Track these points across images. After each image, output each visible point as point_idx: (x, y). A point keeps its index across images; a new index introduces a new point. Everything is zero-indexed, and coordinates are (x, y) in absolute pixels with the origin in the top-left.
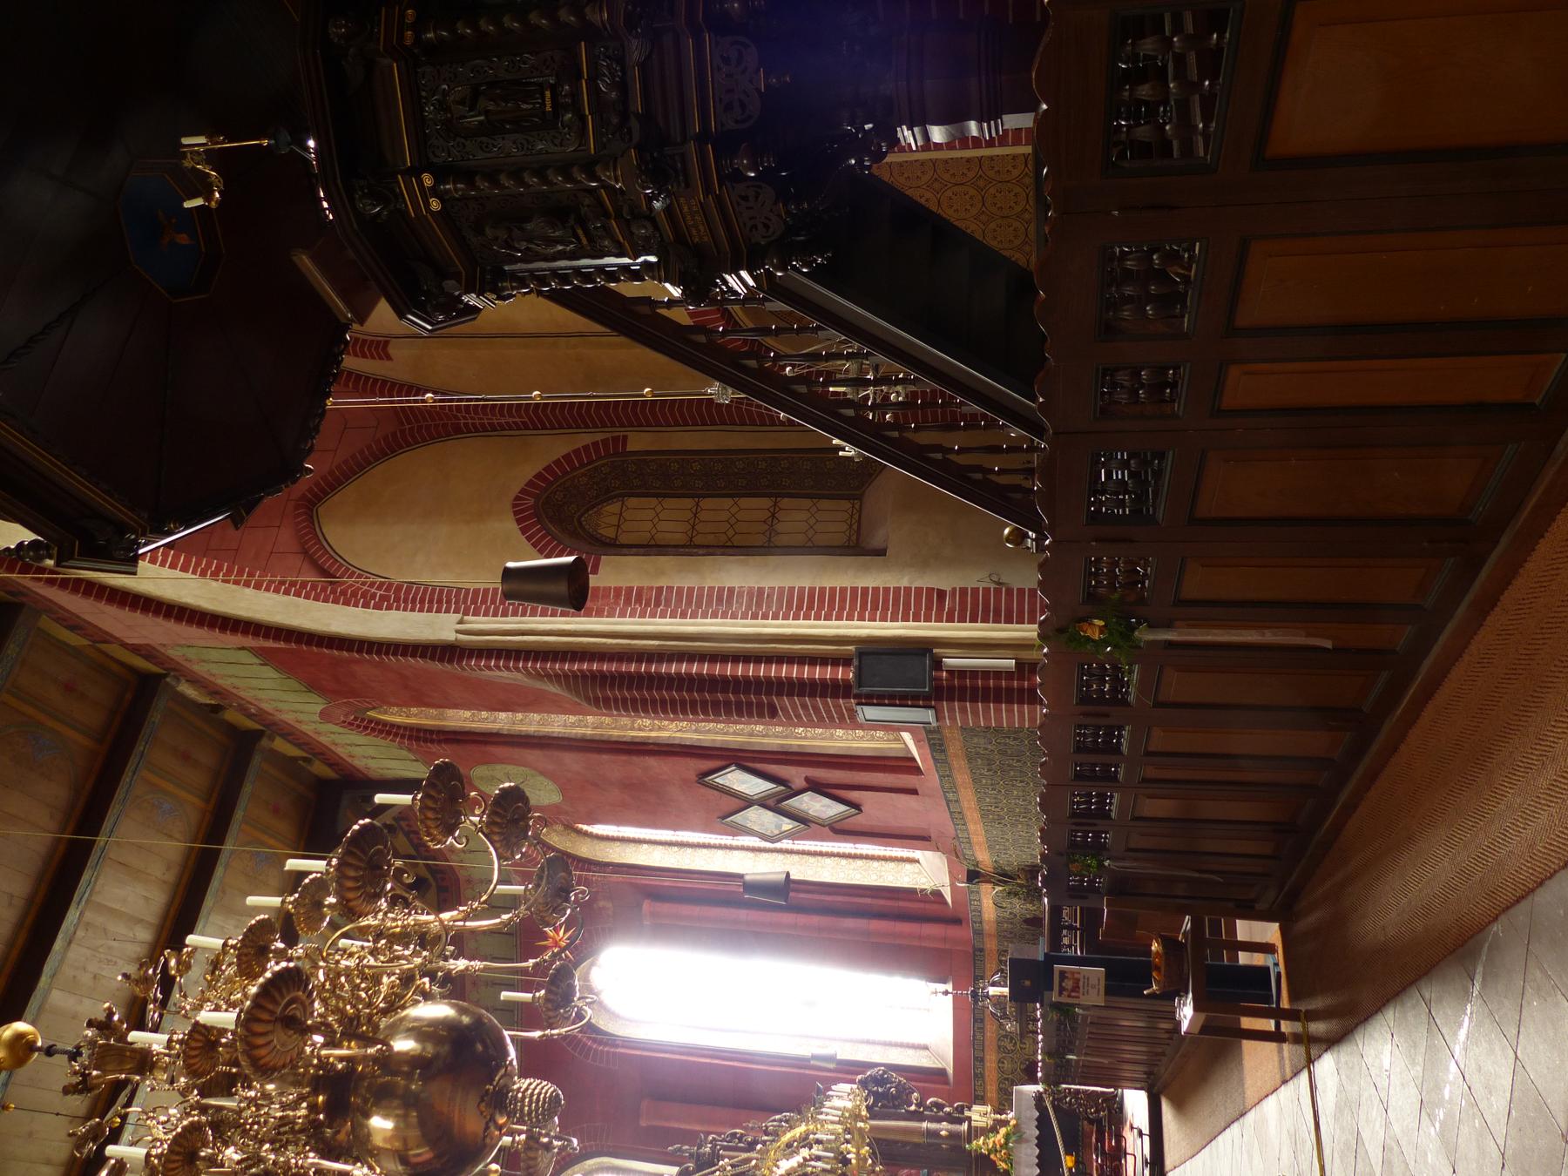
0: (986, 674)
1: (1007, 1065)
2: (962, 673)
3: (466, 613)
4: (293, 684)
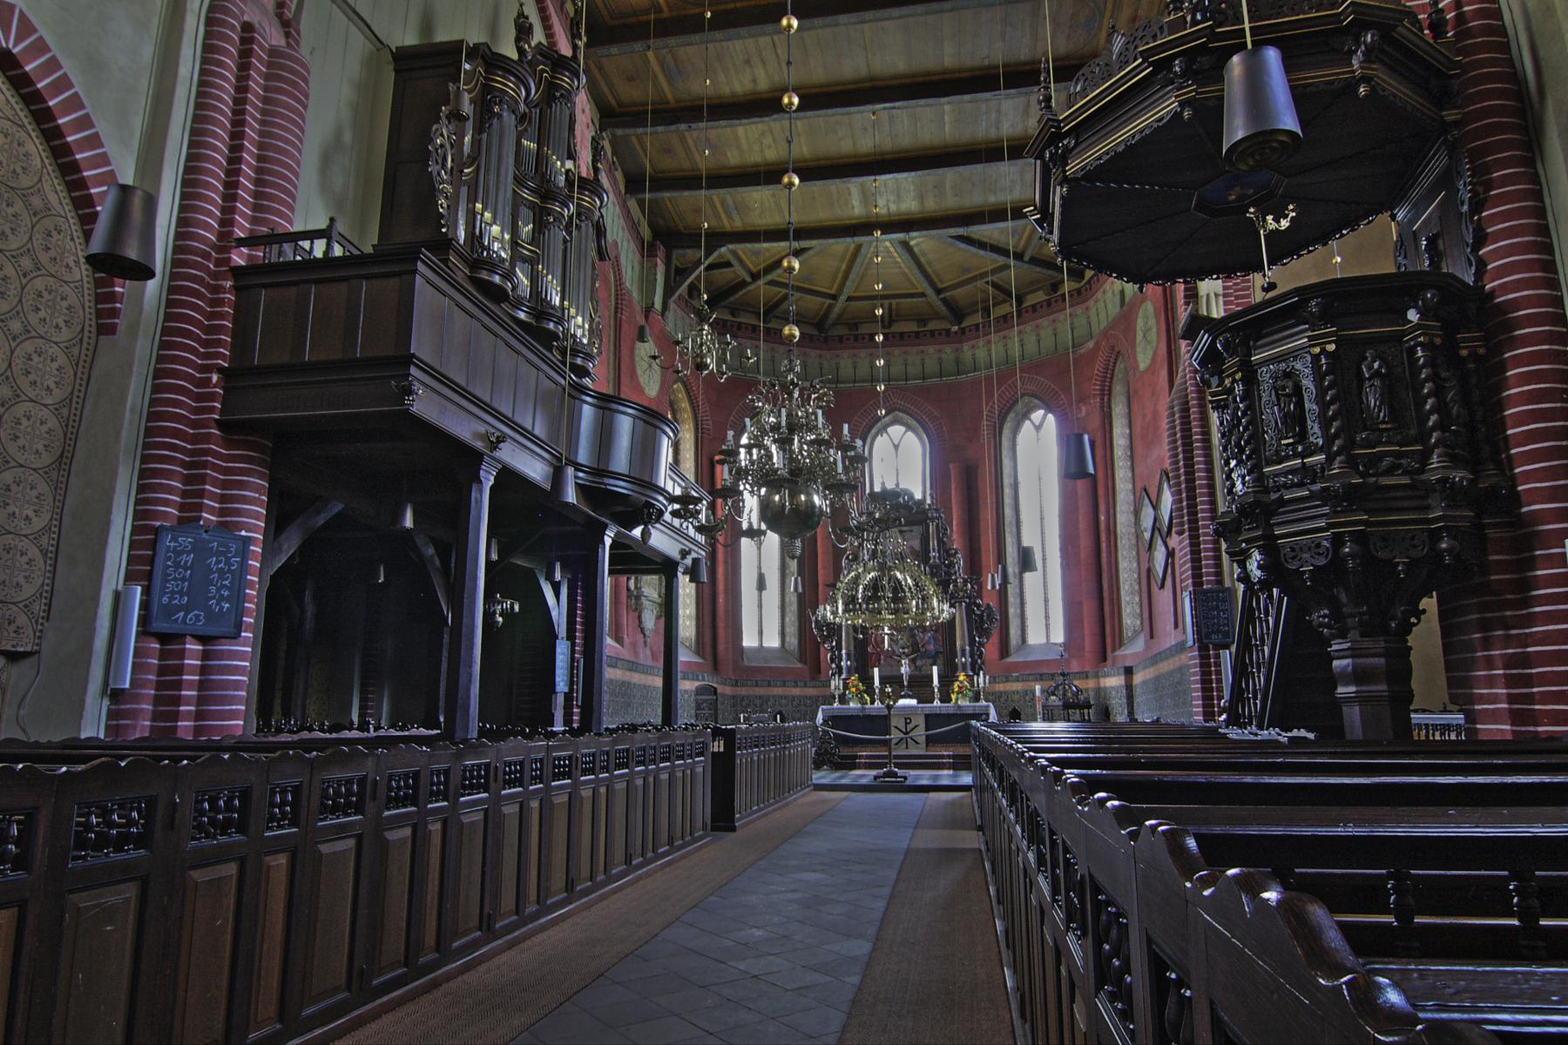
3: (1225, 296)
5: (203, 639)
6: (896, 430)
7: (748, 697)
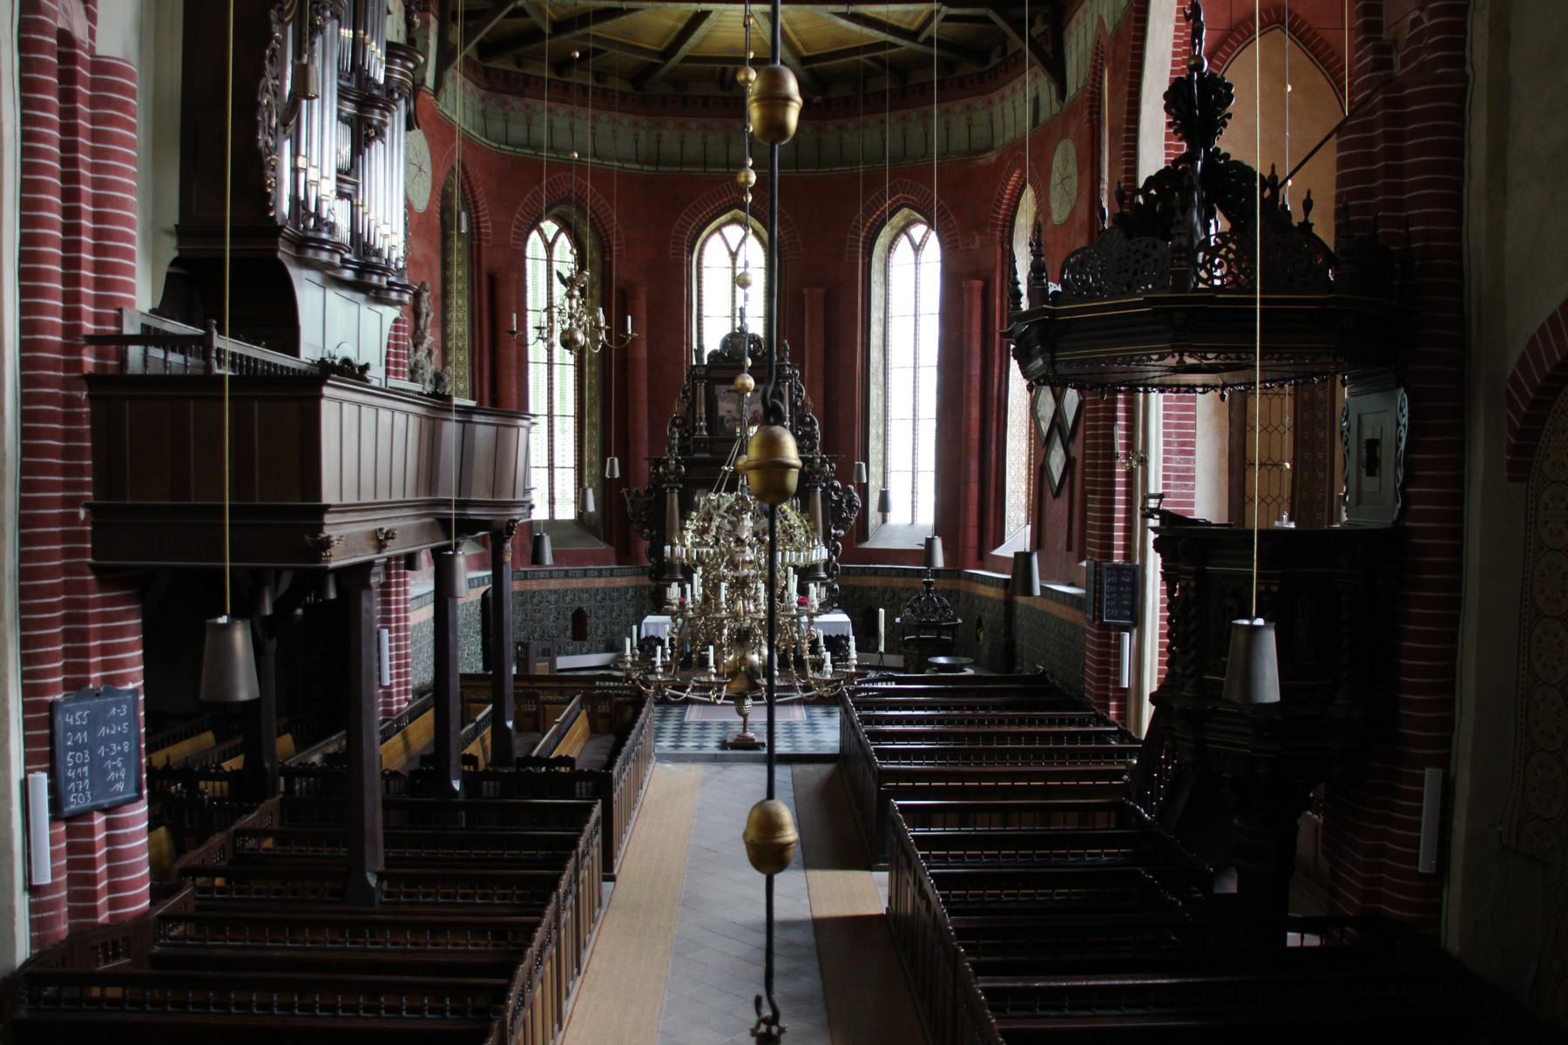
0: (1119, 665)
1: (873, 594)
2: (1119, 647)
4: (1119, 16)
5: (106, 811)
6: (734, 233)
7: (539, 592)
